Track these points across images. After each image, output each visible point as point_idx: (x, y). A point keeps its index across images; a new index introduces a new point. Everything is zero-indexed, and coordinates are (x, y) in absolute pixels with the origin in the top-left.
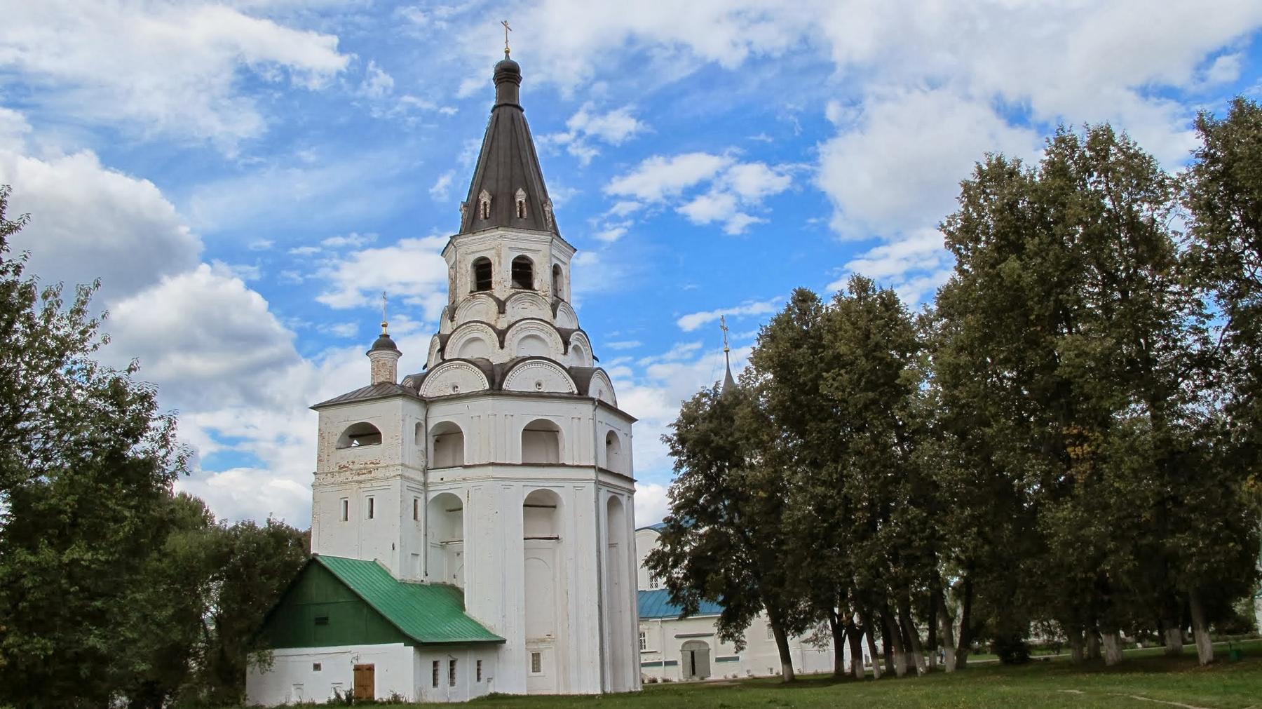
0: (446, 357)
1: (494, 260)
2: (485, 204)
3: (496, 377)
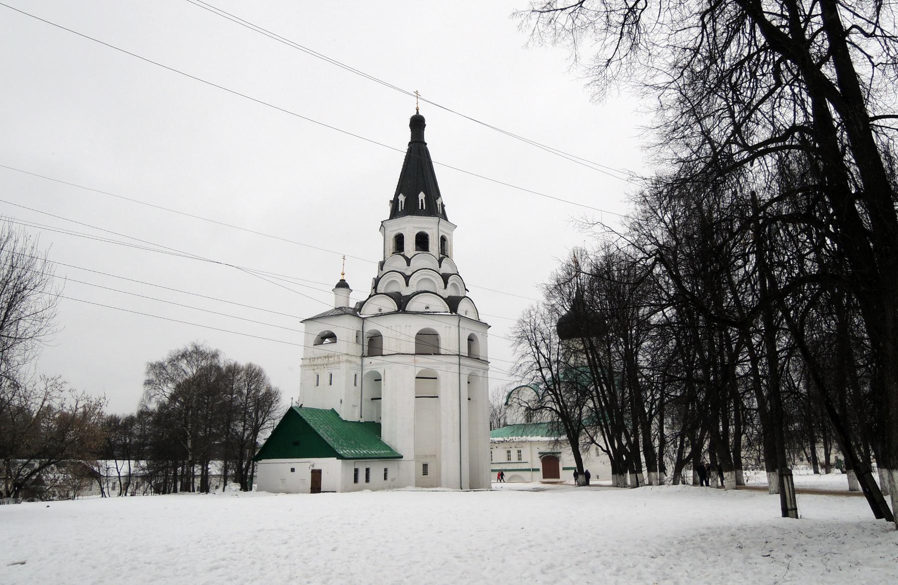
0: (378, 292)
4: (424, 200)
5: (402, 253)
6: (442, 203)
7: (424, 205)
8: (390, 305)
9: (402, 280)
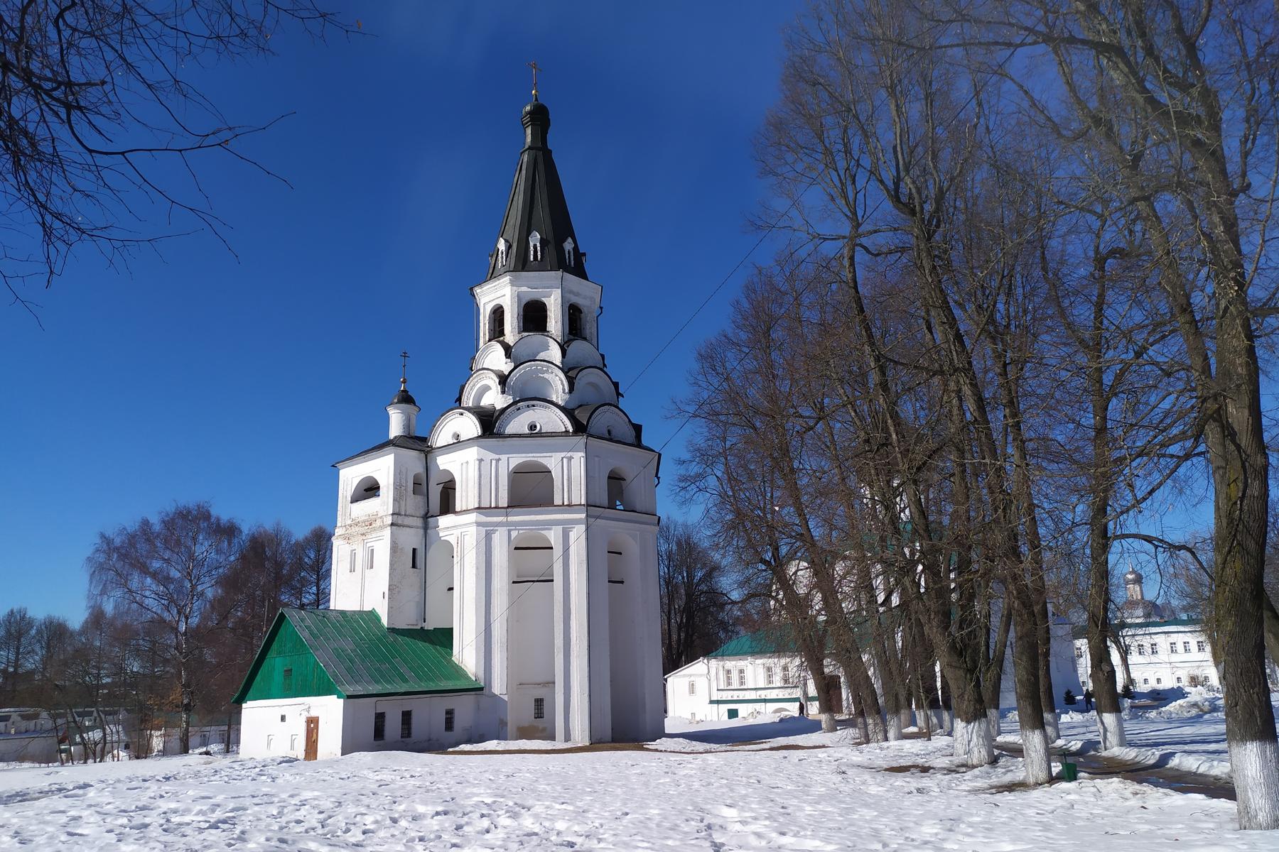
2: (502, 253)
4: (538, 245)
5: (502, 338)
6: (576, 248)
7: (539, 253)
9: (493, 382)
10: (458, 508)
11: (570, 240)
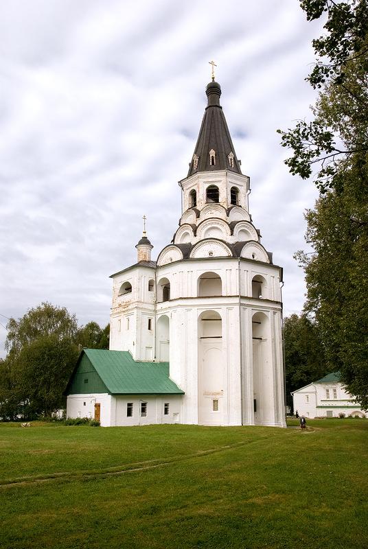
1: (197, 192)
3: (187, 250)
6: (235, 158)
8: (177, 255)
10: (171, 298)
11: (231, 153)
